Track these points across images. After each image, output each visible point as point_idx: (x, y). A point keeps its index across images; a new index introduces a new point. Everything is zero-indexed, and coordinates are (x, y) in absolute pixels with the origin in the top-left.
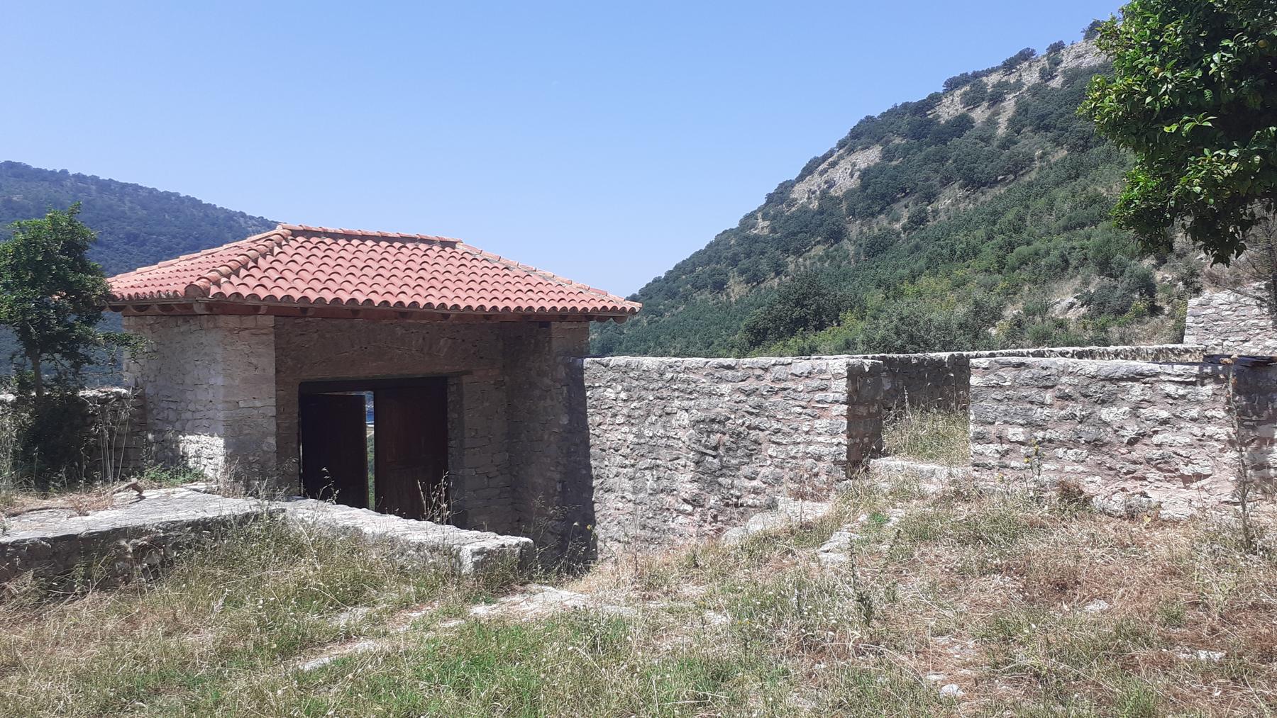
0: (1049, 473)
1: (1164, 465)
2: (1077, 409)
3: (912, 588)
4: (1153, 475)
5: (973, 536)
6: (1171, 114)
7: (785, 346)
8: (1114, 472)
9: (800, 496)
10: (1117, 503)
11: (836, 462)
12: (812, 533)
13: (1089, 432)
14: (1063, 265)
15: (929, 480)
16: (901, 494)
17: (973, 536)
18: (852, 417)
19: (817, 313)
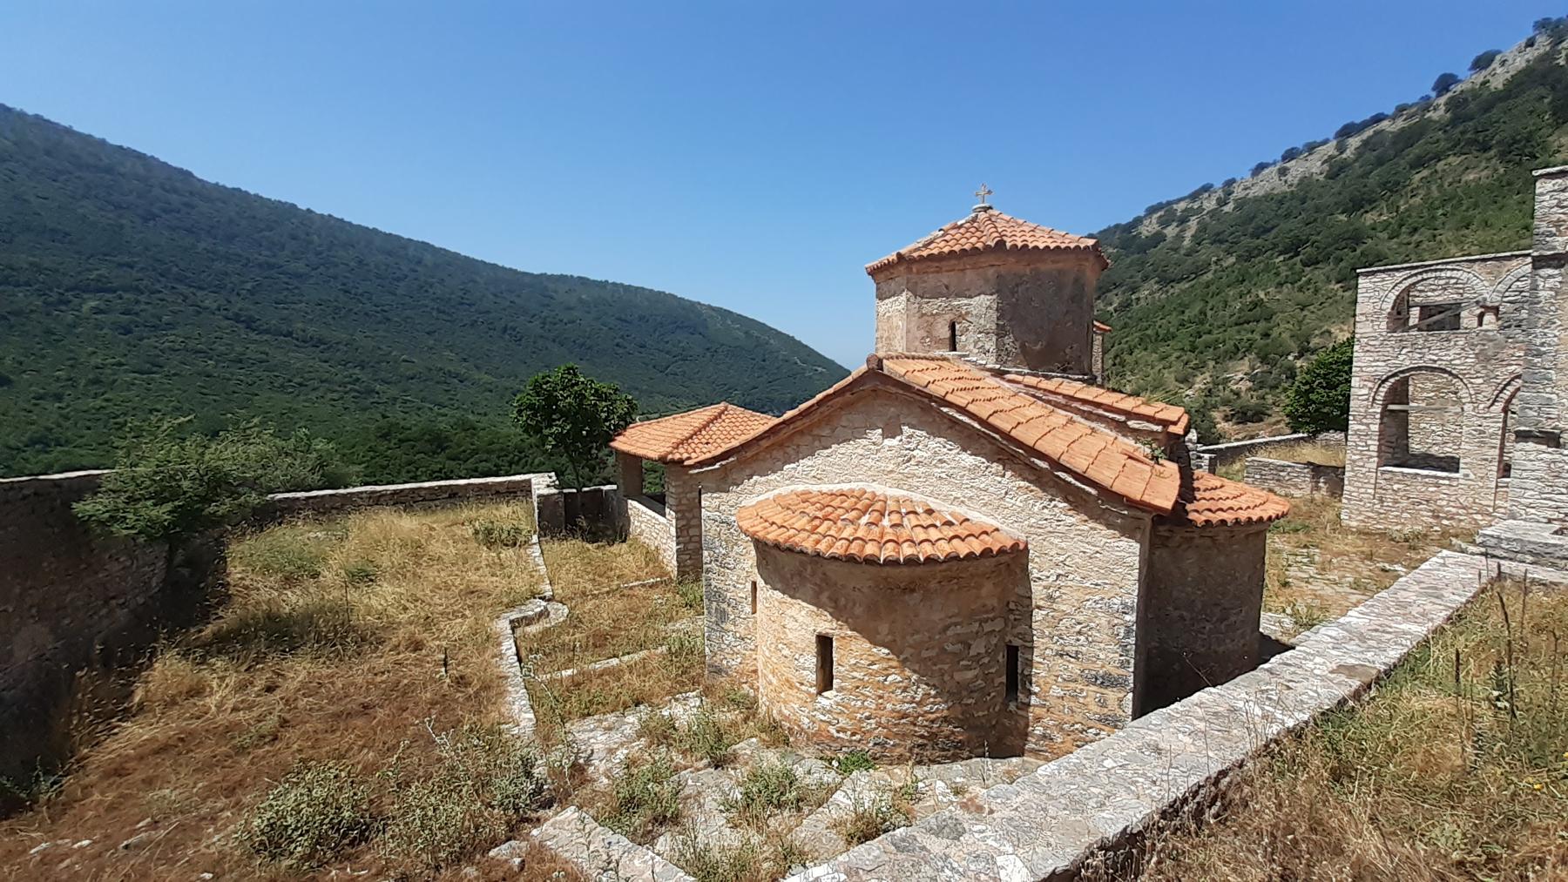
1: (1295, 486)
6: (1300, 417)
13: (1276, 477)
14: (1235, 351)
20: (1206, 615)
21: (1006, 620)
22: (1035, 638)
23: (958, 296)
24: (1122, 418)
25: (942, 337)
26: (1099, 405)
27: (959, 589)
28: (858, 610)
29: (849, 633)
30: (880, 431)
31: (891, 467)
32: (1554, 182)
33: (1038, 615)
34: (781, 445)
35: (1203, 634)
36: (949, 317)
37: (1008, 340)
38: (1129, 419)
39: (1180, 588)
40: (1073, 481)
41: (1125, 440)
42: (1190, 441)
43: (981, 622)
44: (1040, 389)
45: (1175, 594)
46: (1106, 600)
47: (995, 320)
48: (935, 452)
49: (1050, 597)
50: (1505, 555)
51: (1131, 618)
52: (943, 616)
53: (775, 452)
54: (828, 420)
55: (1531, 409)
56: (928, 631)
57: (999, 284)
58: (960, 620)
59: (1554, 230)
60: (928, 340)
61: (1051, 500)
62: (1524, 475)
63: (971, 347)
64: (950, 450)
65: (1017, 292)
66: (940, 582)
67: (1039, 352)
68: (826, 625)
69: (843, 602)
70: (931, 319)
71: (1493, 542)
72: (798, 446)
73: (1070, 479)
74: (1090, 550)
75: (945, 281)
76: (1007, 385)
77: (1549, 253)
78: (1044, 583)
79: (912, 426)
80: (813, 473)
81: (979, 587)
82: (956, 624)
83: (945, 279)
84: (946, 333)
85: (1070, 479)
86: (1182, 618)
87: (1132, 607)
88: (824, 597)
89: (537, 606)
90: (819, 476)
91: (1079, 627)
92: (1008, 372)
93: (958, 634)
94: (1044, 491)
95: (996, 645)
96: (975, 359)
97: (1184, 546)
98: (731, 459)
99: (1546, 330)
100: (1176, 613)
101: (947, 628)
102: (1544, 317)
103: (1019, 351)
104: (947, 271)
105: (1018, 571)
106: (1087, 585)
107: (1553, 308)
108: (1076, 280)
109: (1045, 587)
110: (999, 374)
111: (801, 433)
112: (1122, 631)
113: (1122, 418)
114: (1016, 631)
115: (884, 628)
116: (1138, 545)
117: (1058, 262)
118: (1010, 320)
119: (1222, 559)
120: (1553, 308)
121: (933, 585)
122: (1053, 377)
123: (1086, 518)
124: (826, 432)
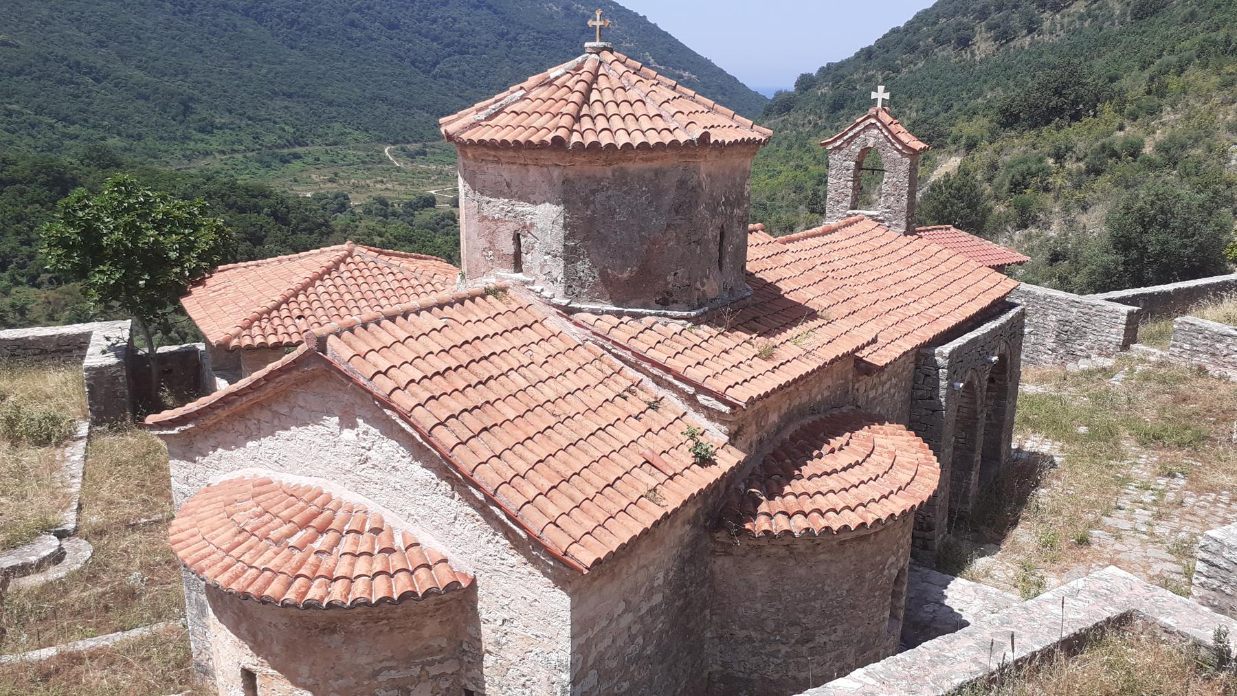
0: (1195, 360)
2: (1209, 342)
3: (1142, 395)
4: (1230, 367)
5: (1163, 381)
7: (1038, 136)
9: (1100, 355)
10: (1216, 374)
12: (1107, 372)
13: (1212, 350)
16: (1142, 361)
17: (1163, 381)
18: (1126, 330)
19: (1075, 103)
20: (782, 636)
21: (461, 661)
22: (487, 686)
23: (523, 198)
24: (691, 390)
25: (506, 252)
26: (668, 370)
27: (391, 630)
28: (277, 649)
29: (271, 671)
30: (336, 419)
31: (348, 466)
33: (488, 660)
34: (241, 416)
35: (777, 658)
36: (513, 226)
37: (583, 267)
38: (697, 392)
39: (747, 604)
40: (506, 520)
41: (696, 416)
42: (941, 354)
43: (424, 665)
44: (609, 340)
45: (741, 611)
46: (545, 654)
47: (563, 241)
48: (388, 458)
49: (498, 643)
50: (1225, 565)
51: (566, 677)
52: (370, 659)
53: (236, 423)
54: (283, 395)
56: (354, 676)
57: (565, 192)
58: (395, 664)
60: (490, 253)
61: (495, 534)
63: (537, 271)
64: (403, 457)
65: (593, 202)
66: (362, 624)
67: (627, 282)
68: (250, 660)
69: (260, 637)
70: (492, 225)
71: (1214, 547)
72: (259, 421)
73: (503, 517)
74: (530, 597)
75: (506, 176)
76: (574, 329)
78: (492, 626)
79: (366, 421)
80: (275, 458)
81: (419, 627)
82: (390, 668)
83: (506, 173)
84: (510, 248)
85: (503, 517)
86: (749, 639)
87: (566, 666)
88: (244, 626)
89: (49, 544)
90: (281, 462)
91: (523, 679)
92: (580, 310)
93: (394, 679)
94: (488, 523)
95: (448, 689)
96: (537, 288)
97: (753, 555)
98: (190, 426)
100: (742, 634)
101: (376, 674)
103: (598, 280)
104: (508, 163)
105: (469, 608)
106: (529, 634)
108: (682, 183)
109: (493, 631)
110: (568, 311)
111: (261, 405)
112: (559, 690)
113: (691, 390)
114: (470, 675)
115: (304, 670)
116: (569, 600)
117: (652, 160)
118: (584, 239)
119: (802, 571)
121: (355, 626)
122: (645, 316)
123: (525, 560)
124: (284, 410)
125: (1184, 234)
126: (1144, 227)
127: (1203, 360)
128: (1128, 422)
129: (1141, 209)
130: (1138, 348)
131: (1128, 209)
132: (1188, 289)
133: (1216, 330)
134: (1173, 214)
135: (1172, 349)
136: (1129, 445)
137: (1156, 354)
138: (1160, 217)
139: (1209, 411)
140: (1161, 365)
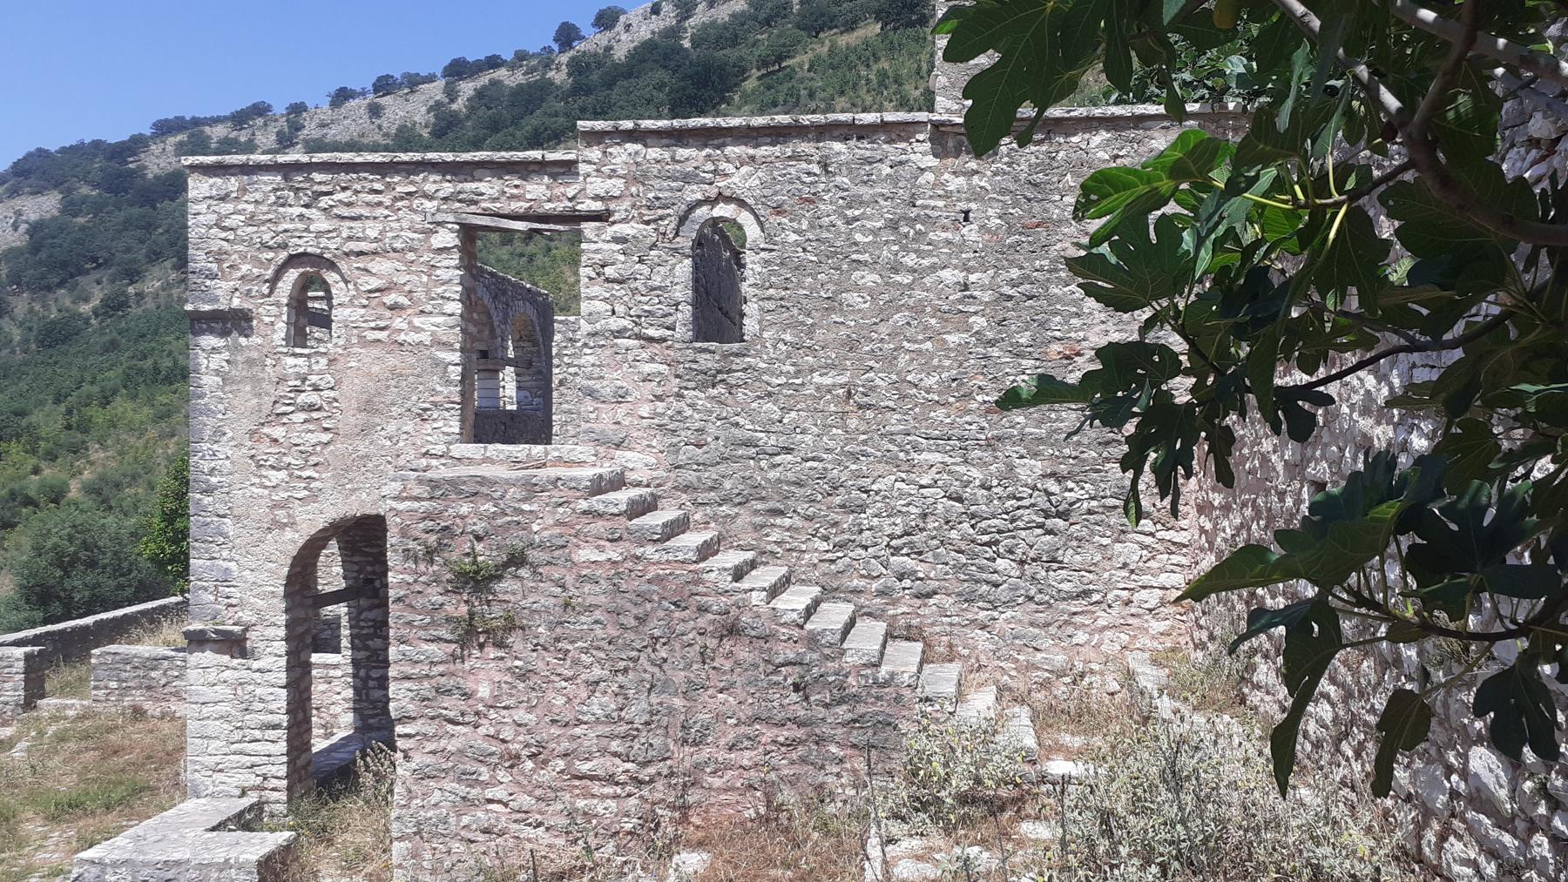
0: (127, 701)
6: (171, 562)
8: (157, 700)
10: (157, 713)
11: (17, 705)
13: (146, 682)
15: (70, 708)
16: (54, 719)
18: (26, 680)
32: (212, 181)
55: (205, 589)
59: (214, 266)
62: (206, 710)
77: (207, 308)
99: (215, 447)
102: (210, 421)
107: (221, 407)
120: (221, 407)
125: (118, 571)
126: (64, 569)
127: (138, 697)
128: (33, 799)
129: (56, 546)
130: (48, 704)
131: (39, 550)
132: (115, 619)
133: (147, 655)
134: (99, 548)
135: (94, 692)
136: (32, 826)
137: (74, 705)
138: (83, 555)
139: (149, 757)
140: (81, 718)
